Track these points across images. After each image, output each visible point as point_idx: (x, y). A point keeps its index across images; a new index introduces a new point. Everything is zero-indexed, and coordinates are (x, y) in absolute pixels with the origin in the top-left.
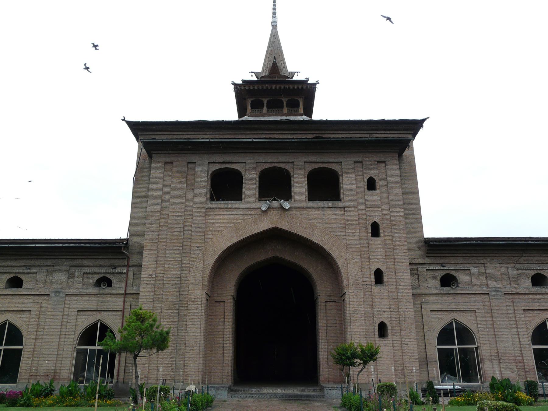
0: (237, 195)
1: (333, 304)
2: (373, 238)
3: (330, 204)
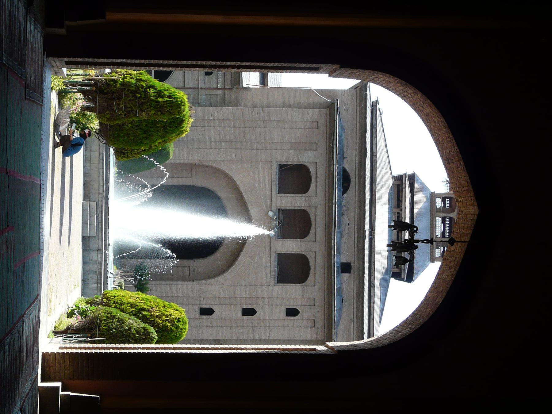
1: (187, 273)
2: (241, 309)
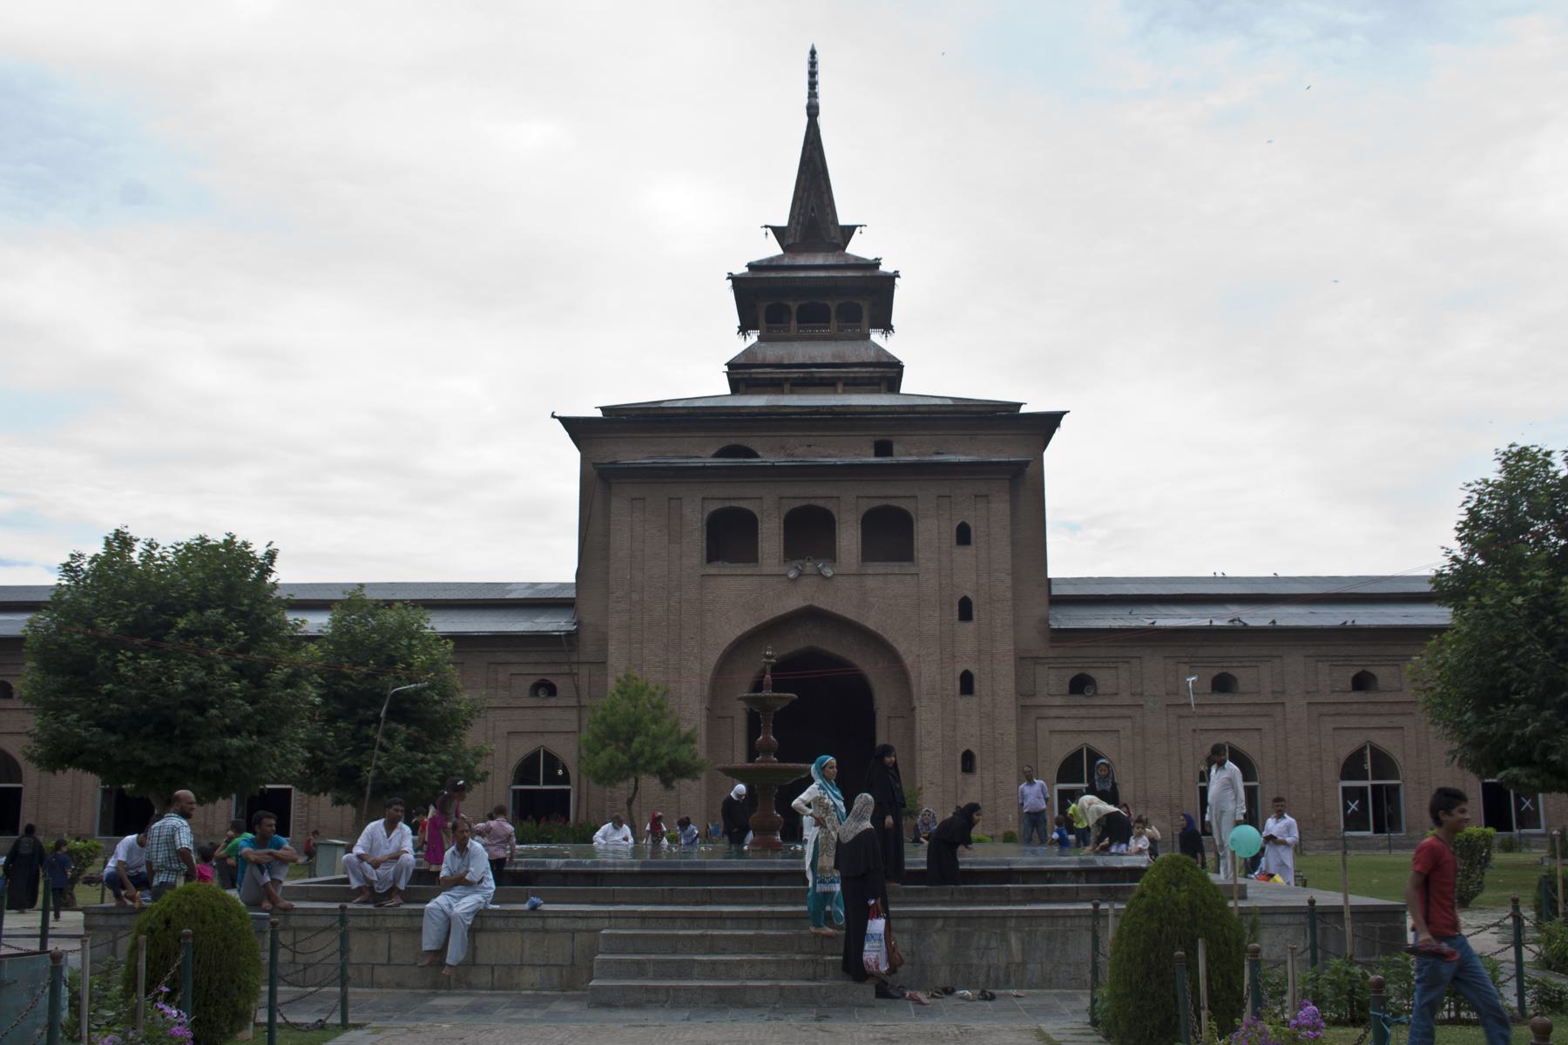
0: (748, 554)
3: (894, 567)
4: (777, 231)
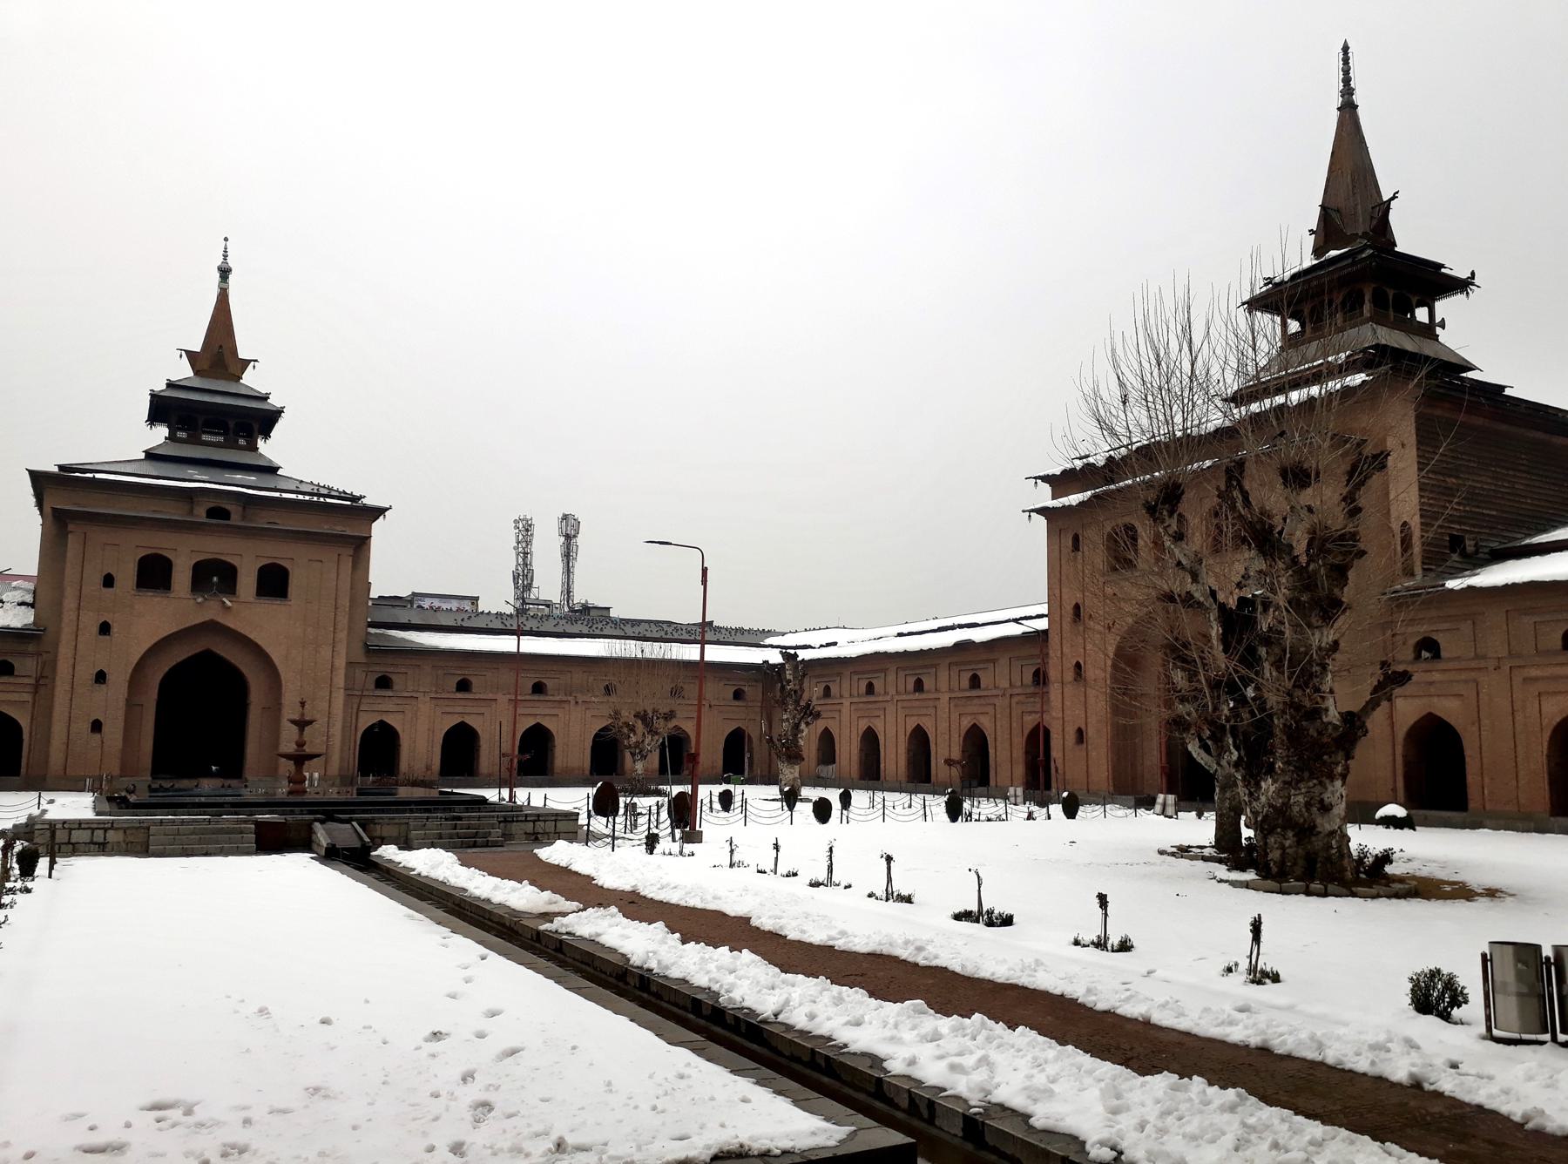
4: (191, 355)
